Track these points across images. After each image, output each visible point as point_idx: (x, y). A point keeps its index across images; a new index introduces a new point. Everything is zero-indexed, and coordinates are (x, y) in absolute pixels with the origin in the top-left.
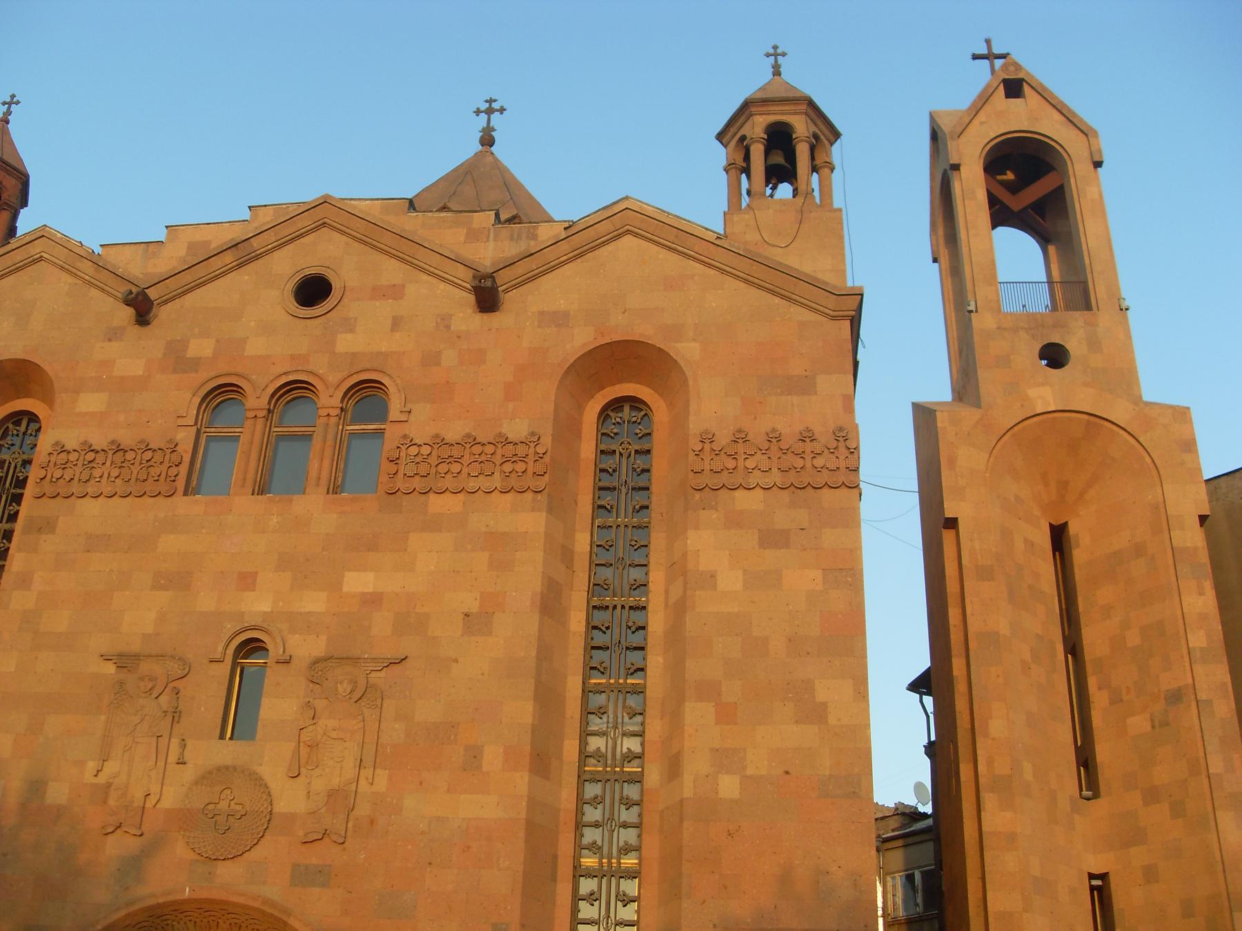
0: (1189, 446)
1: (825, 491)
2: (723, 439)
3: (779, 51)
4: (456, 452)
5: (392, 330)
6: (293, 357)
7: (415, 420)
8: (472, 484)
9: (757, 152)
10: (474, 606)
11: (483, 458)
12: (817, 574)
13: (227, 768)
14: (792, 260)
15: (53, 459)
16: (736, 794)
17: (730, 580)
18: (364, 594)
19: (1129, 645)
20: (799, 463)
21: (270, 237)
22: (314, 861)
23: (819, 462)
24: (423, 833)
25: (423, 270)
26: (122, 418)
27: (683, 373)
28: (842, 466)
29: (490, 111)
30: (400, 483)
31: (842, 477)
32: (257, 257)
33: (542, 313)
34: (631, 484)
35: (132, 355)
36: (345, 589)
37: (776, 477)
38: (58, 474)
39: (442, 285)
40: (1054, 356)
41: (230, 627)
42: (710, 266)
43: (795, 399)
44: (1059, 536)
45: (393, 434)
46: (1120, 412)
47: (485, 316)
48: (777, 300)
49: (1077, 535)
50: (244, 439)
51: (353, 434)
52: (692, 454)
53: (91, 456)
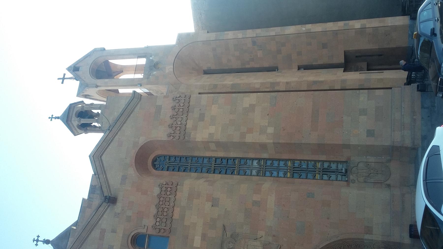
0: (188, 35)
1: (190, 103)
2: (170, 131)
3: (51, 117)
4: (160, 210)
5: (116, 232)
7: (147, 225)
8: (172, 204)
10: (210, 204)
12: (213, 106)
14: (121, 110)
16: (273, 128)
23: (182, 105)
27: (148, 142)
28: (184, 98)
29: (37, 241)
34: (179, 162)
36: (199, 246)
37: (185, 116)
39: (104, 216)
42: (117, 133)
47: (118, 202)
48: (132, 115)
52: (174, 140)
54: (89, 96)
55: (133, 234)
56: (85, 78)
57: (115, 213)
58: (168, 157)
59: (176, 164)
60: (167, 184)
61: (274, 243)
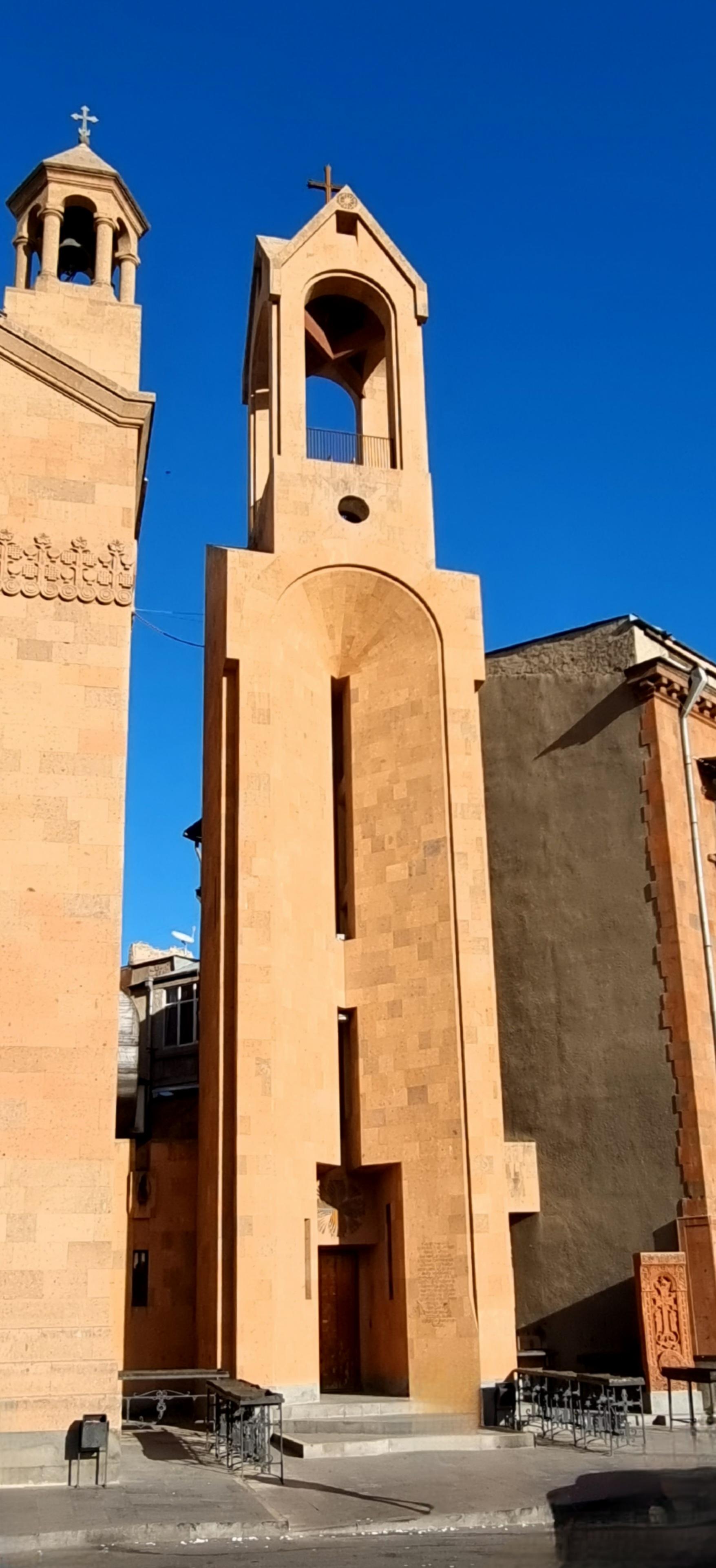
9: (53, 227)
20: (69, 574)
23: (90, 575)
40: (353, 510)
44: (340, 692)
49: (357, 689)
56: (309, 255)
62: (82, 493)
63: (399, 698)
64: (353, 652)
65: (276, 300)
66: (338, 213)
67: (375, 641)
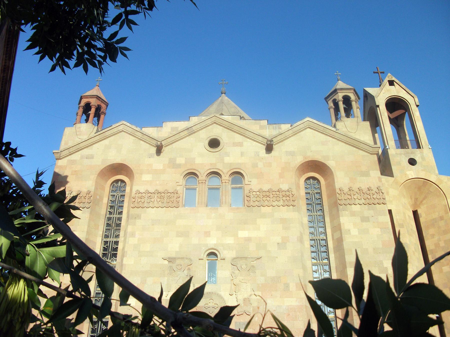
1: (377, 205)
2: (346, 190)
5: (241, 156)
6: (211, 164)
7: (252, 183)
8: (274, 204)
10: (280, 241)
11: (276, 196)
12: (379, 229)
13: (210, 293)
15: (137, 195)
17: (354, 232)
18: (245, 238)
19: (441, 246)
20: (369, 197)
21: (198, 126)
22: (242, 321)
24: (275, 310)
25: (248, 138)
26: (158, 182)
30: (252, 203)
31: (382, 201)
32: (195, 133)
33: (286, 152)
35: (158, 163)
36: (239, 236)
37: (363, 201)
38: (139, 200)
39: (255, 143)
40: (412, 162)
41: (204, 249)
43: (365, 178)
45: (247, 188)
46: (433, 178)
48: (355, 149)
50: (197, 189)
51: (233, 188)
52: (337, 194)
53: (149, 195)
54: (367, 99)
55: (242, 172)
57: (259, 152)
58: (319, 191)
59: (314, 201)
60: (293, 195)
61: (252, 309)
62: (366, 174)
63: (435, 215)
64: (416, 202)
65: (378, 106)
66: (389, 81)
67: (424, 199)
